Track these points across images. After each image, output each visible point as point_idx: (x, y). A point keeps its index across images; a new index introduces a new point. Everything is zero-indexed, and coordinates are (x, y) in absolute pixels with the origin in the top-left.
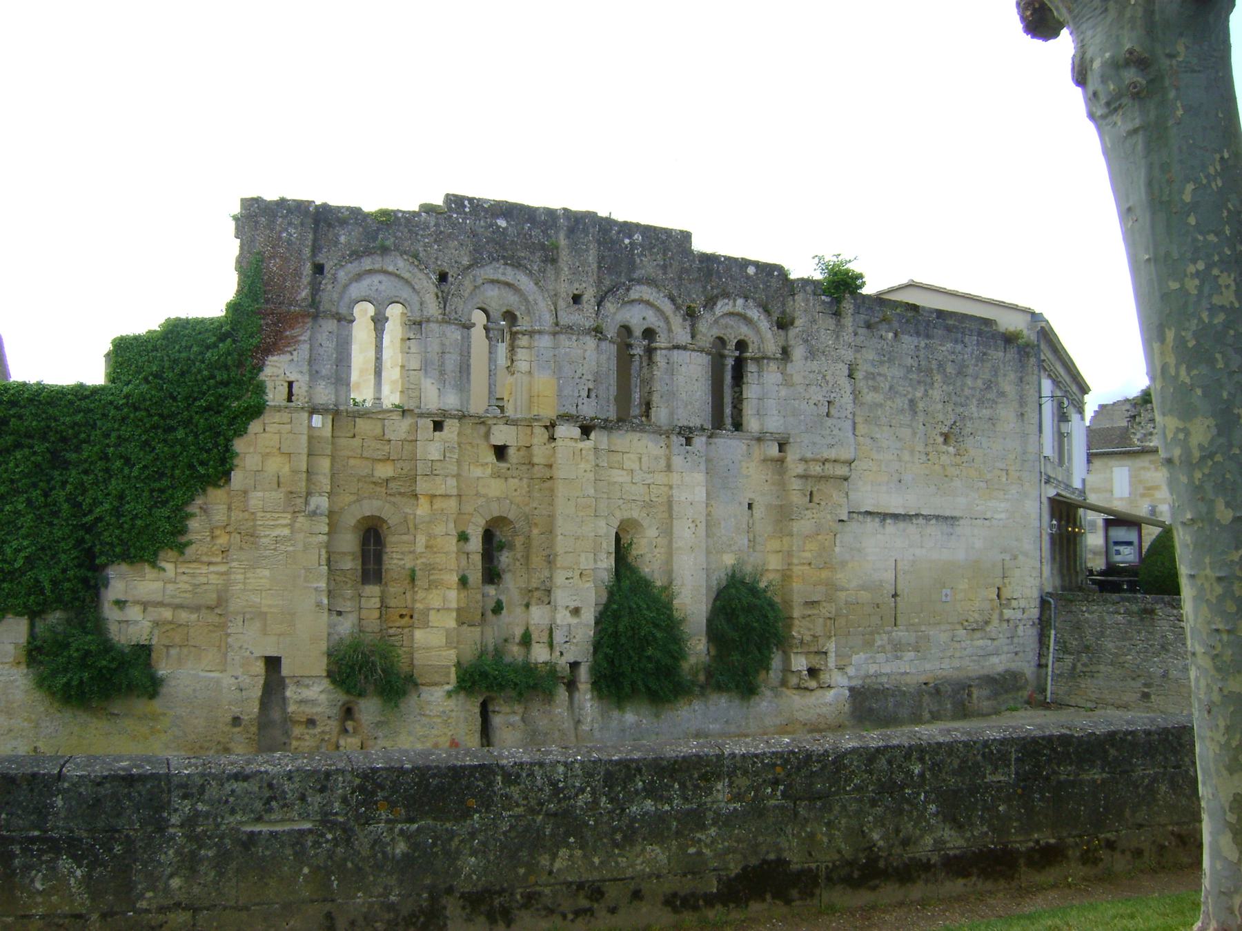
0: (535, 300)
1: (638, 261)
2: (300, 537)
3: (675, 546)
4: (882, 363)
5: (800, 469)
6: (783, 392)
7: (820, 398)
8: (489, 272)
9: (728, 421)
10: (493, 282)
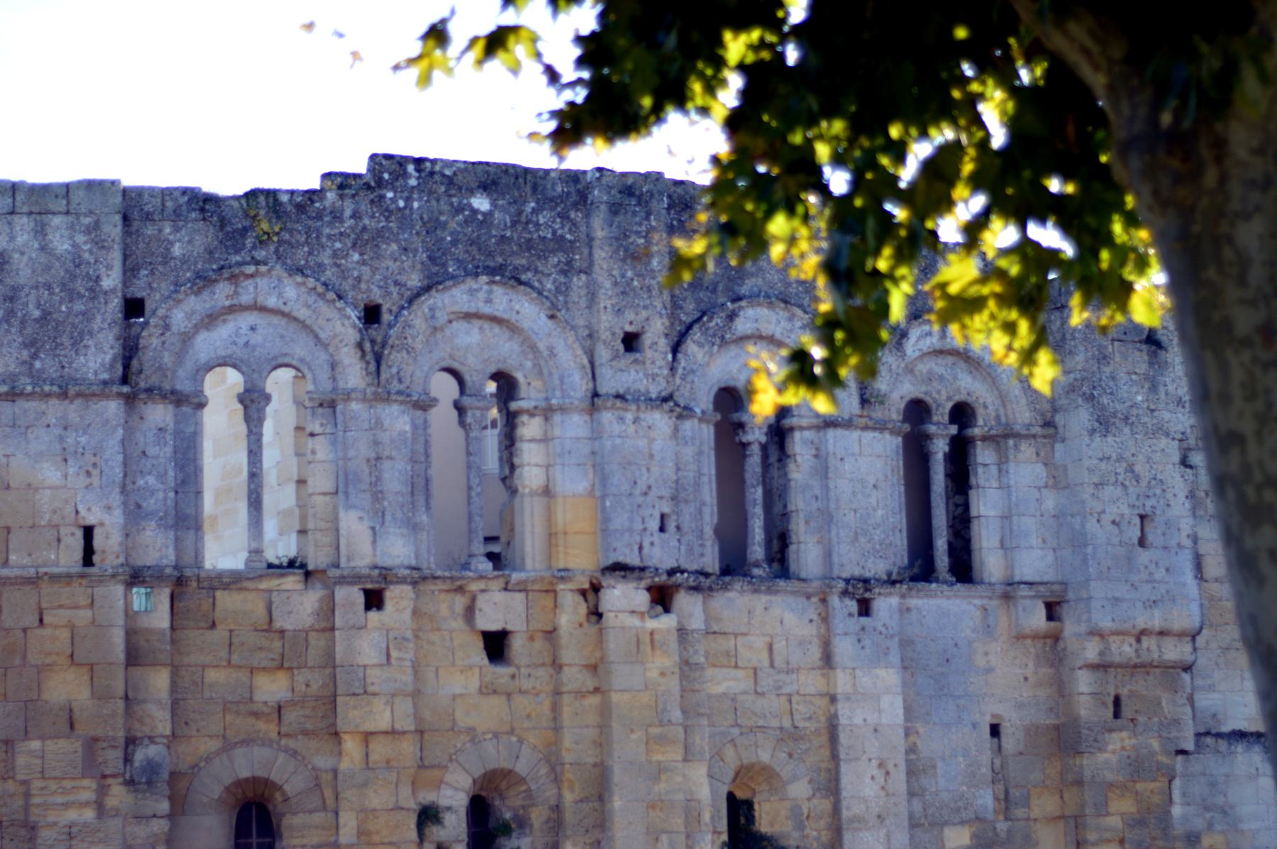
0: (551, 349)
2: (114, 824)
3: (845, 814)
5: (1091, 651)
6: (1050, 502)
7: (1126, 510)
8: (457, 297)
9: (942, 560)
10: (468, 316)
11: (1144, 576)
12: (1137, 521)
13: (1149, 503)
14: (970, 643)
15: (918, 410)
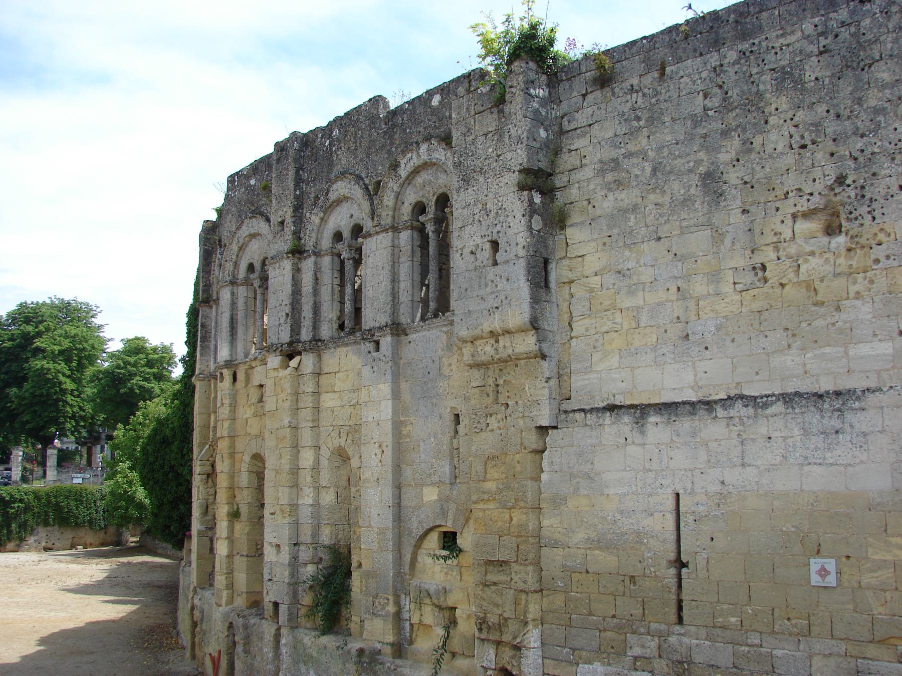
4: (632, 133)
7: (478, 240)
12: (488, 246)
14: (440, 358)
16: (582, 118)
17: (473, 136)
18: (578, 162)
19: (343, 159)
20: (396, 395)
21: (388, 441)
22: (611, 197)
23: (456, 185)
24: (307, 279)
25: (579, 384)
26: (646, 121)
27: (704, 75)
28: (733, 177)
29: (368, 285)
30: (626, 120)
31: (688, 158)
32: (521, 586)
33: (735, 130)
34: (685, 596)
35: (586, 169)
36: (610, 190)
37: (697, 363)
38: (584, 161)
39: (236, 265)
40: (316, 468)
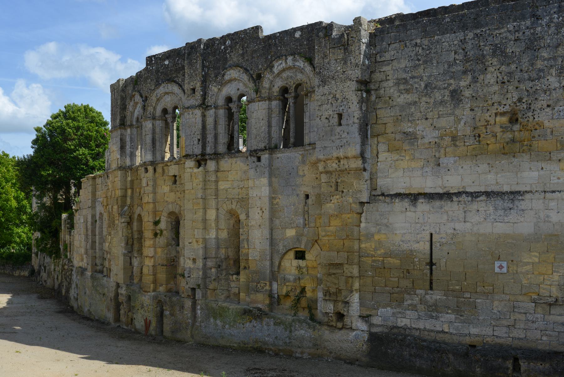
1: (228, 56)
4: (416, 67)
7: (331, 113)
11: (337, 137)
12: (336, 116)
13: (341, 108)
14: (297, 167)
15: (285, 90)
16: (387, 56)
17: (328, 60)
18: (385, 78)
19: (234, 58)
20: (270, 184)
21: (266, 206)
22: (402, 97)
23: (318, 84)
24: (210, 121)
25: (382, 183)
26: (423, 62)
27: (455, 42)
28: (467, 93)
29: (252, 127)
30: (412, 60)
31: (444, 82)
32: (349, 274)
33: (470, 71)
34: (434, 278)
35: (389, 82)
36: (402, 93)
37: (444, 176)
38: (388, 78)
39: (155, 109)
40: (217, 219)
